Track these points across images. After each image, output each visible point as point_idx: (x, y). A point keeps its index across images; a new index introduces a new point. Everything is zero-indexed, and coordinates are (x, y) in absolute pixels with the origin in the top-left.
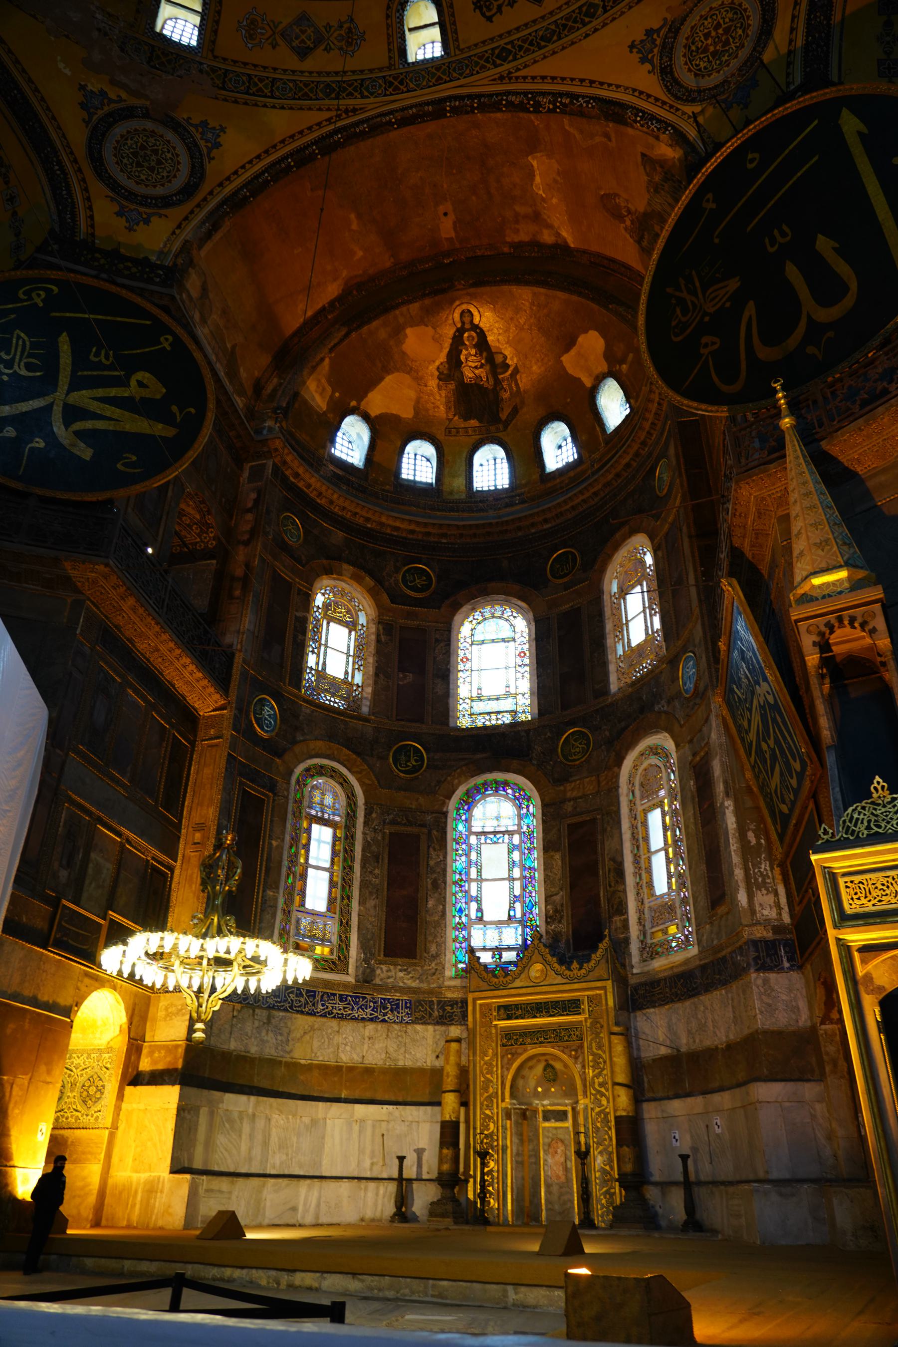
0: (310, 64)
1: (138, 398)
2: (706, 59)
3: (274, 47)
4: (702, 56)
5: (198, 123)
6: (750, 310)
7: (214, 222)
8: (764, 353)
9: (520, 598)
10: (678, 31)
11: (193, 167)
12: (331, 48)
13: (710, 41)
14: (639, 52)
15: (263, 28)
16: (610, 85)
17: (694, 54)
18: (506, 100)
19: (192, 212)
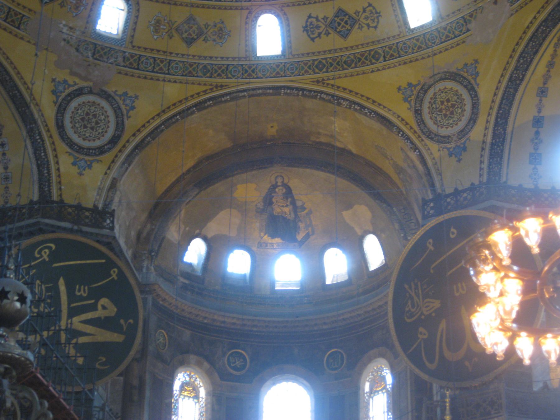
0: (195, 49)
1: (103, 318)
2: (441, 116)
3: (171, 37)
4: (439, 113)
5: (121, 94)
6: (443, 325)
7: (129, 160)
8: (447, 354)
9: (306, 379)
10: (426, 92)
11: (117, 124)
12: (207, 39)
13: (443, 107)
14: (403, 93)
15: (165, 25)
16: (385, 107)
17: (434, 110)
18: (320, 96)
19: (116, 156)
